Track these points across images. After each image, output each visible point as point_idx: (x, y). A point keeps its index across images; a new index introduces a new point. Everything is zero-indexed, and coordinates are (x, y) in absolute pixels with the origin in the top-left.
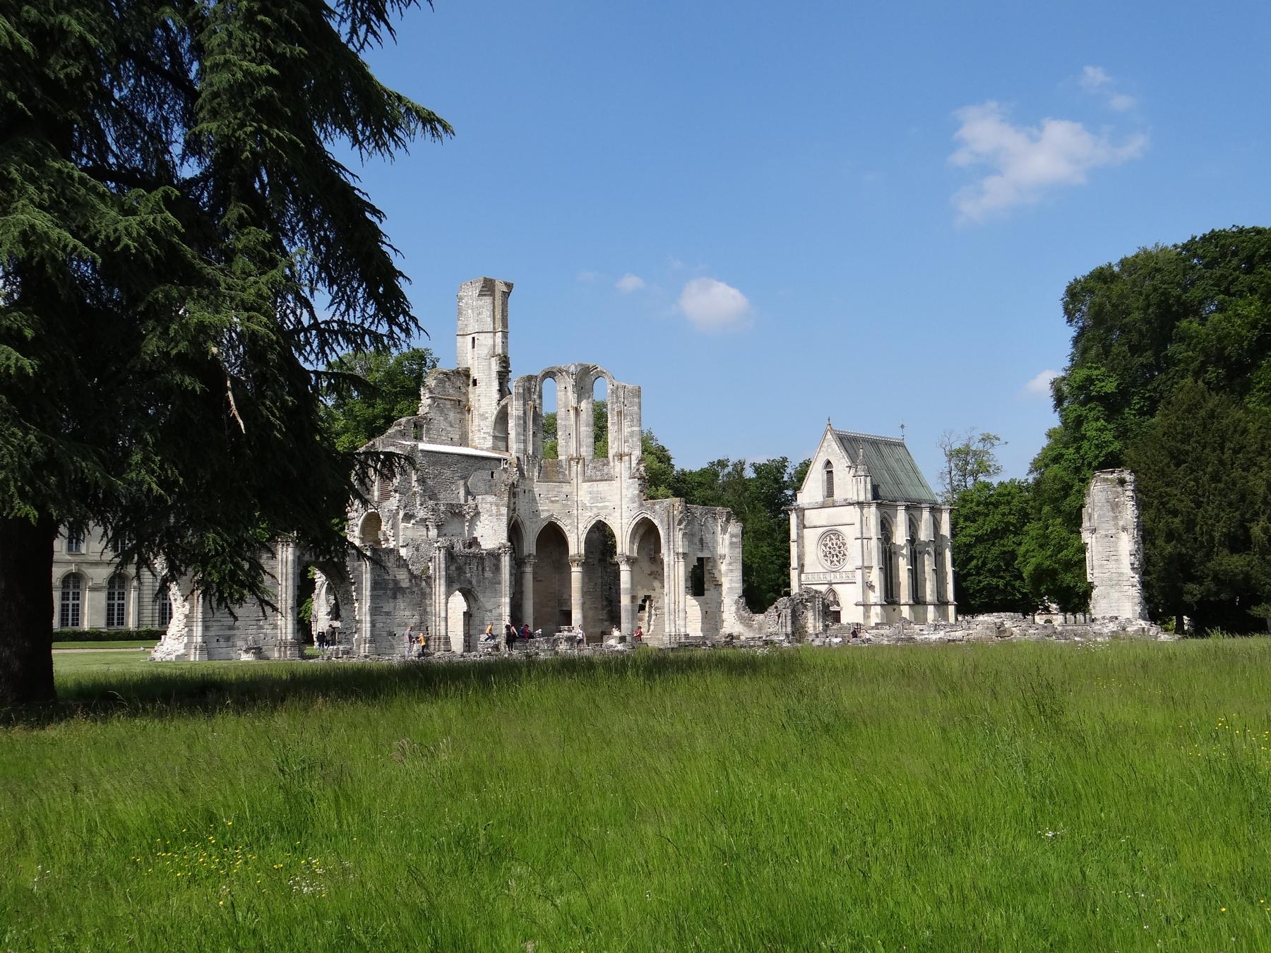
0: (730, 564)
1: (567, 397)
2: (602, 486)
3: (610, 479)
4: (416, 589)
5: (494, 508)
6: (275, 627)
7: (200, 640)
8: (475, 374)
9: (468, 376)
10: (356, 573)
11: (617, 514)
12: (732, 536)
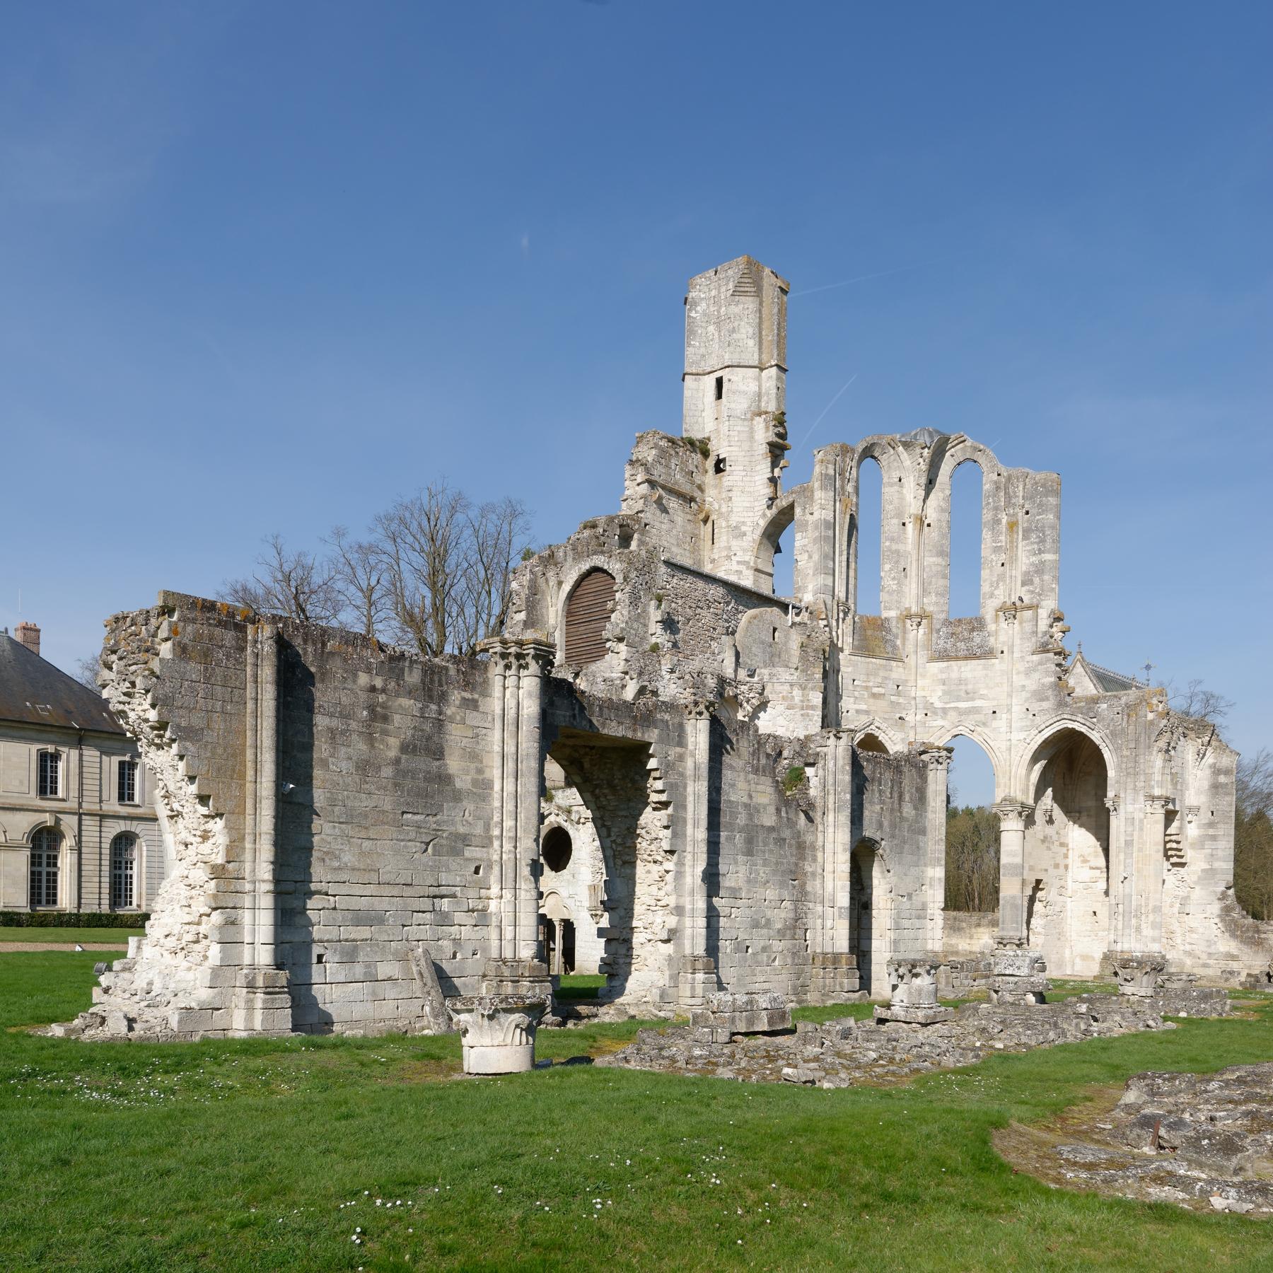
0: (1211, 825)
1: (902, 499)
2: (970, 669)
3: (986, 654)
4: (787, 833)
5: (797, 692)
6: (482, 917)
7: (265, 956)
8: (719, 448)
9: (706, 454)
10: (673, 778)
11: (1001, 723)
12: (1217, 771)
